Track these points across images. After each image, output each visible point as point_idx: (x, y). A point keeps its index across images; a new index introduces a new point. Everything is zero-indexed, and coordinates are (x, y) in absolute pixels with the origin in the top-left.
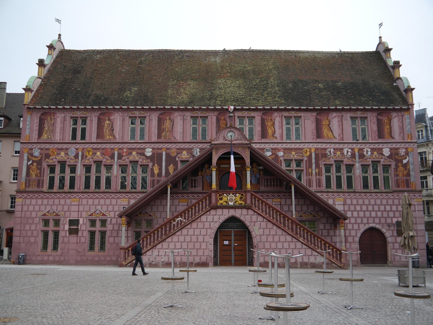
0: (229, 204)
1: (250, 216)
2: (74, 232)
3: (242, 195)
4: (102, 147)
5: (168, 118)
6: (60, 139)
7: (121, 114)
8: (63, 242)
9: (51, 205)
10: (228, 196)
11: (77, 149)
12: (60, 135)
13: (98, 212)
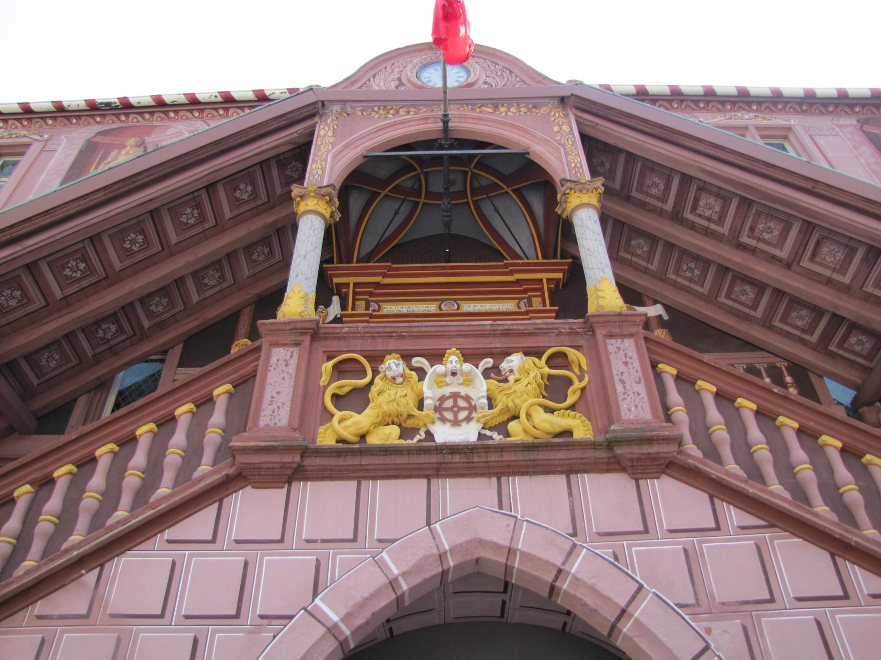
0: (429, 435)
1: (676, 546)
3: (558, 360)
10: (421, 373)
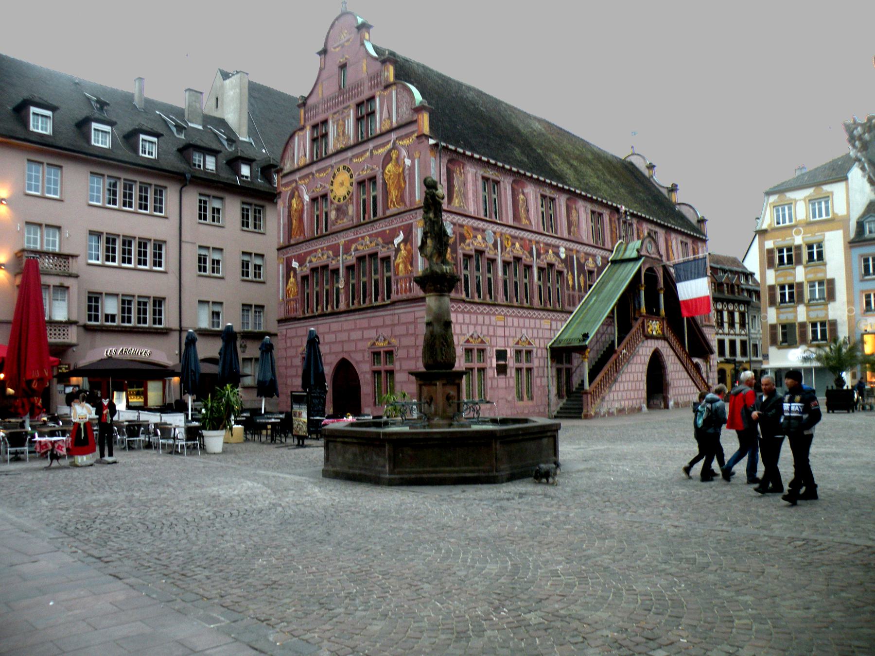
2: (502, 370)
4: (521, 235)
5: (574, 206)
6: (474, 211)
7: (533, 188)
8: (492, 388)
9: (475, 325)
11: (495, 233)
12: (474, 205)
13: (524, 339)
